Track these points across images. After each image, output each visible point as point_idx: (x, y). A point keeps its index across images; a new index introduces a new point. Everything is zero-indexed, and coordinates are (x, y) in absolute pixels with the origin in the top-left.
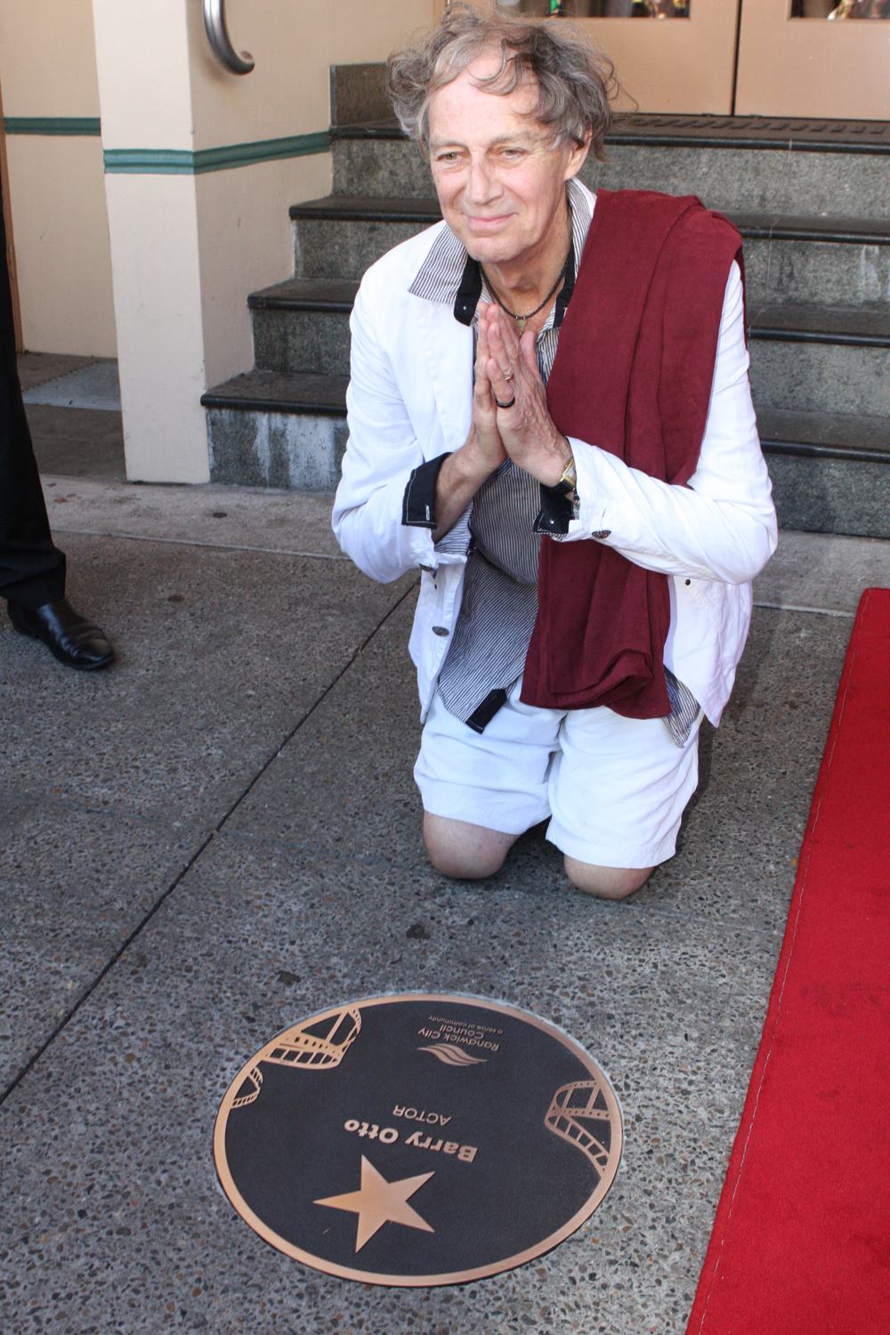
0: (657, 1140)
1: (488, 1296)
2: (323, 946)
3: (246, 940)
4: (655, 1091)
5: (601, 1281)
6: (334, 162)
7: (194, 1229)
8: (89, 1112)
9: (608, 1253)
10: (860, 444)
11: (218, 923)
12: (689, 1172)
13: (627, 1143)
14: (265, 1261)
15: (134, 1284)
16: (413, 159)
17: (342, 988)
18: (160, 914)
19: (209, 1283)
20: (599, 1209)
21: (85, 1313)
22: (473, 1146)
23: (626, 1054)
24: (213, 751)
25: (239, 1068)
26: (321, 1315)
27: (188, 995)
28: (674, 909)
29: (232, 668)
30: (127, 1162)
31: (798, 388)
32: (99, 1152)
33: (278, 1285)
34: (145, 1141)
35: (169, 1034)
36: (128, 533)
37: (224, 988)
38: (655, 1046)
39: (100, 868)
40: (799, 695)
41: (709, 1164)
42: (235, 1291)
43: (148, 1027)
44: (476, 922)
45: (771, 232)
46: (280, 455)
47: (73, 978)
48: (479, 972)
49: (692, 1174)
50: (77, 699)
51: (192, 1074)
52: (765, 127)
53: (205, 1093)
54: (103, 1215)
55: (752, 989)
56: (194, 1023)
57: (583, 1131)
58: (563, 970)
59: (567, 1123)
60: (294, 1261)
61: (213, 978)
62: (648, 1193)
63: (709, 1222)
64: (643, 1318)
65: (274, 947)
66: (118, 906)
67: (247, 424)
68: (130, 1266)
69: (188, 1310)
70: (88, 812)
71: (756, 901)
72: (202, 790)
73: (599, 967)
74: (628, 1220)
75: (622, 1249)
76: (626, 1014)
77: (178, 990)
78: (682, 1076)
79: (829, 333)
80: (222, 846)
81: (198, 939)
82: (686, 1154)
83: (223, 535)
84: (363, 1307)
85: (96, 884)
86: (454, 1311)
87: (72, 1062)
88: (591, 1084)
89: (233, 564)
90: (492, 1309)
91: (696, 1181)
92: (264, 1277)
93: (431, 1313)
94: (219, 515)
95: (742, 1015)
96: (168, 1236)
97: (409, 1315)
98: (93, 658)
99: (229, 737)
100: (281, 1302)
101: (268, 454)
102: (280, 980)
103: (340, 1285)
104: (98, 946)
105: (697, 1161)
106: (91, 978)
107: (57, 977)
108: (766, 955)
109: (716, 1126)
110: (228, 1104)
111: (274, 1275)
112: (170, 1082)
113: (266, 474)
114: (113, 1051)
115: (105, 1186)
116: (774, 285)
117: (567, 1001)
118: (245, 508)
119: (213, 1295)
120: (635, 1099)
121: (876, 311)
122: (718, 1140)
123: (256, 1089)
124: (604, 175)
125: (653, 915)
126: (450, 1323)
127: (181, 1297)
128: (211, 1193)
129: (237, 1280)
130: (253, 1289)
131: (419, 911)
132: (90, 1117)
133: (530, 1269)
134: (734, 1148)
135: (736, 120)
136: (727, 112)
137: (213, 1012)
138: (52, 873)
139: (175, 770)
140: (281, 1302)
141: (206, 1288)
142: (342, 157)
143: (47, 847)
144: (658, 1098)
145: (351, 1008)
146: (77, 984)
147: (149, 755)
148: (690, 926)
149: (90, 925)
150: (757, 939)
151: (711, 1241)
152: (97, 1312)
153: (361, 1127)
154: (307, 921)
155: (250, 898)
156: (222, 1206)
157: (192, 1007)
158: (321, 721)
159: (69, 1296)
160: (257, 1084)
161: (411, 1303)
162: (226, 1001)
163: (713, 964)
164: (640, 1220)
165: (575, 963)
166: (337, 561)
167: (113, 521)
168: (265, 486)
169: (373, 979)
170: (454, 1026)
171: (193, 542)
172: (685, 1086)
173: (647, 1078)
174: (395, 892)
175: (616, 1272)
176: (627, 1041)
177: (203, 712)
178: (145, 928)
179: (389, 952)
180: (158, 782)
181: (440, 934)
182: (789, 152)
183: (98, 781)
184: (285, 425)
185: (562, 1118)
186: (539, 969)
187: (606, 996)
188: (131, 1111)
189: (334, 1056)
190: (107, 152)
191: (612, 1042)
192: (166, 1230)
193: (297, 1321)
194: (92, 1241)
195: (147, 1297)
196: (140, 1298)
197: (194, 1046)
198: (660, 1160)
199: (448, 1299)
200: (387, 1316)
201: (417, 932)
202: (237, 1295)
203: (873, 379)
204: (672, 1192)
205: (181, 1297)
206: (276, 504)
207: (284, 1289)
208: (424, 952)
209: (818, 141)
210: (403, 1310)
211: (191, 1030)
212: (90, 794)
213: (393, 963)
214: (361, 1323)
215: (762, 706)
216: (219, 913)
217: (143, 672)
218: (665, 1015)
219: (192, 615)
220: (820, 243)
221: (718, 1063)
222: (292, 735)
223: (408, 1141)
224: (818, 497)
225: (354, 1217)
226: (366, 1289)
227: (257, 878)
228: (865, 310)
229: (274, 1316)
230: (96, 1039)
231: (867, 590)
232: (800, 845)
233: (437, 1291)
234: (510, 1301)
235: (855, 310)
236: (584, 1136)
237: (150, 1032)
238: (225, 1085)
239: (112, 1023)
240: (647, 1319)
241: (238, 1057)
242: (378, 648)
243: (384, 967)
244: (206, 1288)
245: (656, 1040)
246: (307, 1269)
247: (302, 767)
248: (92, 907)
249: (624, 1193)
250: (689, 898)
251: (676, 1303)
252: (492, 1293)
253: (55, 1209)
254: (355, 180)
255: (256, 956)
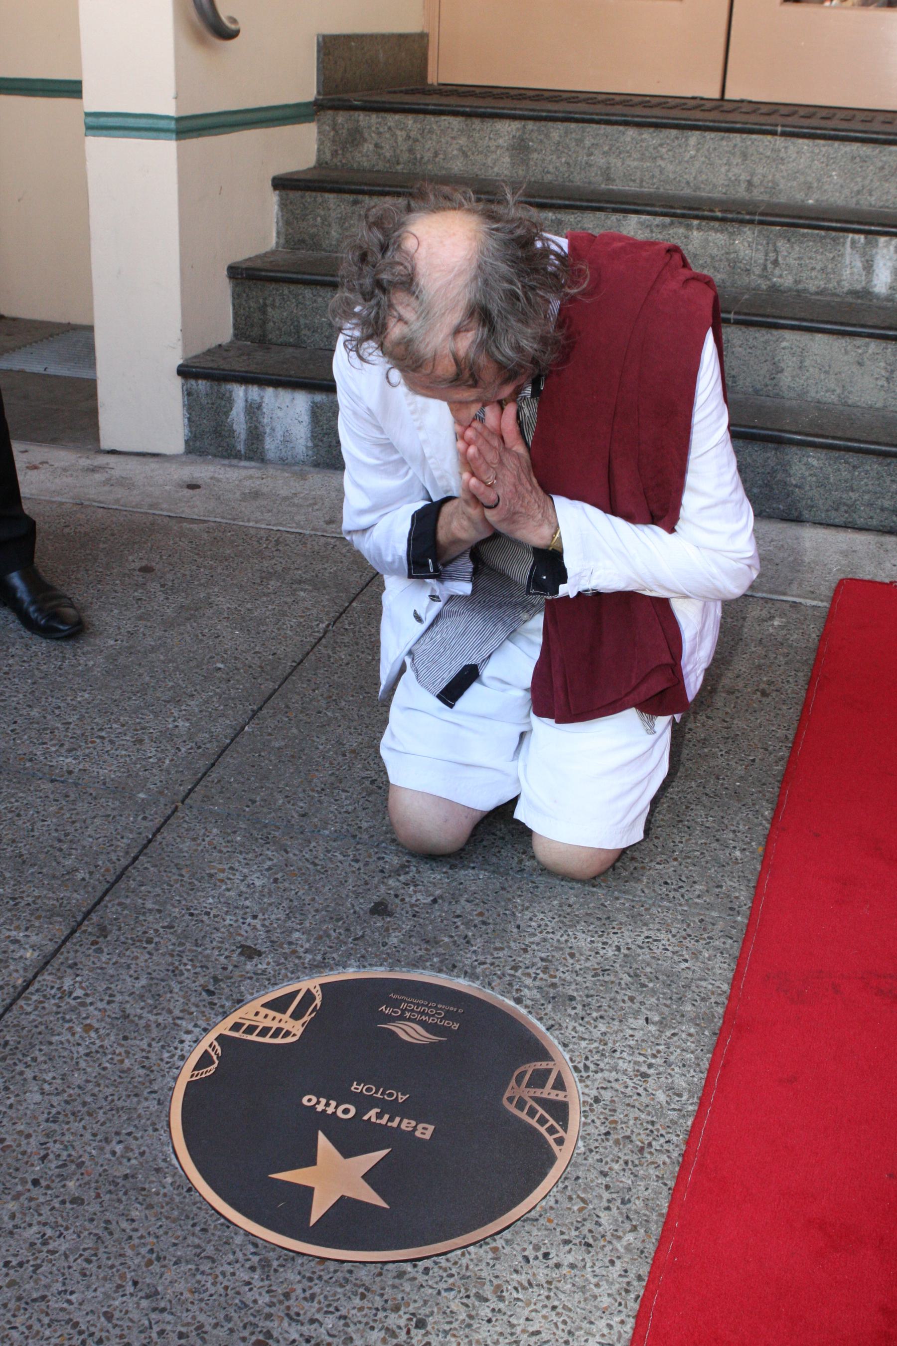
0: (615, 1122)
1: (441, 1272)
2: (285, 921)
3: (208, 914)
4: (614, 1073)
5: (555, 1261)
6: (319, 132)
7: (148, 1200)
8: (45, 1081)
9: (562, 1233)
10: (839, 434)
11: (181, 896)
12: (646, 1155)
13: (585, 1124)
14: (218, 1233)
15: (86, 1254)
16: (399, 133)
17: (303, 963)
18: (122, 884)
19: (162, 1254)
20: (555, 1189)
21: (36, 1282)
22: (431, 1124)
23: (586, 1036)
24: (180, 723)
25: (197, 1041)
26: (274, 1288)
27: (148, 967)
28: (639, 893)
29: (202, 640)
30: (81, 1131)
31: (779, 375)
32: (54, 1122)
33: (231, 1257)
34: (101, 1111)
35: (128, 1006)
36: (100, 502)
37: (185, 960)
38: (616, 1028)
39: (62, 838)
40: (770, 683)
41: (666, 1146)
42: (187, 1262)
43: (107, 998)
44: (440, 901)
45: (757, 218)
46: (256, 428)
47: (33, 947)
48: (441, 950)
49: (649, 1156)
51: (150, 1045)
52: (754, 111)
53: (163, 1064)
54: (57, 1184)
55: (714, 974)
56: (153, 994)
57: (541, 1111)
58: (525, 951)
59: (525, 1103)
60: (247, 1234)
61: (173, 950)
62: (605, 1174)
63: (664, 1204)
64: (595, 1297)
65: (237, 921)
66: (79, 876)
68: (82, 1236)
69: (140, 1280)
70: (52, 781)
71: (721, 887)
72: (167, 762)
73: (562, 949)
74: (583, 1200)
75: (577, 1229)
76: (588, 996)
77: (138, 961)
78: (641, 1059)
79: (812, 321)
80: (187, 818)
81: (159, 911)
82: (643, 1137)
83: (196, 506)
84: (316, 1281)
85: (58, 853)
86: (407, 1287)
87: (30, 1031)
88: (550, 1065)
89: (205, 536)
90: (445, 1286)
91: (653, 1163)
92: (217, 1249)
93: (383, 1289)
94: (193, 486)
95: (703, 999)
96: (122, 1207)
97: (361, 1290)
98: (61, 627)
99: (197, 710)
100: (233, 1274)
101: (244, 426)
102: (241, 954)
103: (293, 1259)
104: (59, 915)
105: (654, 1143)
106: (51, 947)
107: (17, 946)
108: (730, 941)
109: (674, 1110)
110: (186, 1075)
111: (227, 1247)
112: (127, 1052)
113: (241, 447)
114: (70, 1021)
115: (59, 1155)
116: (757, 270)
117: (528, 981)
118: (219, 480)
119: (164, 1266)
120: (594, 1081)
121: (859, 301)
122: (676, 1123)
123: (214, 1063)
124: (591, 154)
125: (617, 899)
126: (403, 1299)
127: (133, 1267)
128: (166, 1165)
129: (190, 1252)
130: (205, 1261)
131: (383, 888)
132: (46, 1087)
133: (484, 1247)
134: (691, 1132)
135: (725, 103)
136: (716, 95)
137: (173, 984)
138: (14, 841)
139: (141, 741)
140: (233, 1274)
141: (158, 1259)
142: (327, 128)
143: (10, 815)
144: (617, 1080)
145: (312, 983)
146: (36, 954)
147: (115, 726)
148: (654, 910)
149: (51, 895)
150: (720, 925)
151: (665, 1223)
152: (48, 1281)
153: (318, 1102)
154: (270, 896)
155: (212, 871)
156: (177, 1178)
157: (152, 979)
158: (289, 695)
159: (21, 1265)
160: (215, 1057)
161: (364, 1278)
162: (186, 974)
163: (676, 949)
164: (596, 1201)
165: (538, 944)
167: (86, 490)
168: (240, 459)
169: (334, 955)
170: (414, 1004)
171: (165, 513)
172: (644, 1069)
173: (606, 1060)
174: (359, 869)
175: (570, 1251)
176: (588, 1023)
177: (171, 684)
178: (107, 898)
179: (352, 929)
180: (124, 752)
181: (403, 912)
182: (778, 138)
183: (63, 751)
184: (262, 398)
185: (521, 1098)
186: (502, 949)
187: (568, 978)
188: (88, 1081)
189: (294, 1031)
190: (88, 115)
191: (573, 1024)
192: (120, 1201)
193: (249, 1294)
194: (45, 1210)
195: (99, 1267)
196: (92, 1267)
197: (153, 1018)
198: (617, 1142)
199: (401, 1275)
200: (339, 1290)
201: (380, 909)
202: (190, 1266)
203: (855, 368)
204: (628, 1173)
205: (133, 1267)
207: (237, 1262)
208: (387, 930)
209: (808, 128)
210: (355, 1285)
211: (150, 1001)
212: (54, 763)
213: (355, 939)
214: (313, 1297)
215: (733, 693)
216: (182, 886)
217: (112, 642)
218: (626, 998)
219: (163, 586)
220: (806, 231)
221: (678, 1047)
222: (260, 709)
223: (366, 1118)
224: (796, 486)
225: (310, 1191)
226: (318, 1263)
227: (220, 851)
228: (850, 299)
229: (226, 1288)
230: (55, 1008)
231: (842, 581)
232: (767, 832)
233: (390, 1266)
234: (463, 1277)
235: (839, 300)
236: (542, 1116)
237: (109, 1003)
238: (183, 1058)
239: (70, 993)
240: (599, 1299)
241: (197, 1030)
242: (350, 624)
243: (346, 943)
244: (158, 1259)
245: (616, 1023)
246: (260, 1242)
247: (270, 741)
248: (54, 877)
249: (580, 1174)
250: (654, 882)
251: (628, 1283)
252: (445, 1270)
253: (8, 1178)
254: (340, 152)
255: (217, 929)
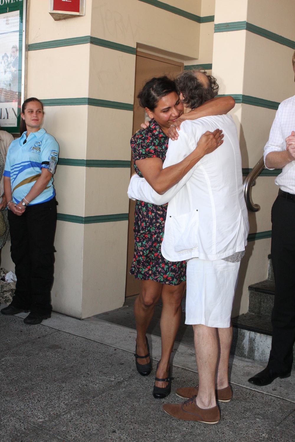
29: (217, 434)
46: (252, 347)
50: (159, 436)
67: (242, 334)
101: (248, 346)
113: (246, 353)
166: (266, 394)
167: (188, 363)
168: (245, 358)
184: (255, 337)
206: (248, 366)
217: (185, 429)
242: (274, 436)
